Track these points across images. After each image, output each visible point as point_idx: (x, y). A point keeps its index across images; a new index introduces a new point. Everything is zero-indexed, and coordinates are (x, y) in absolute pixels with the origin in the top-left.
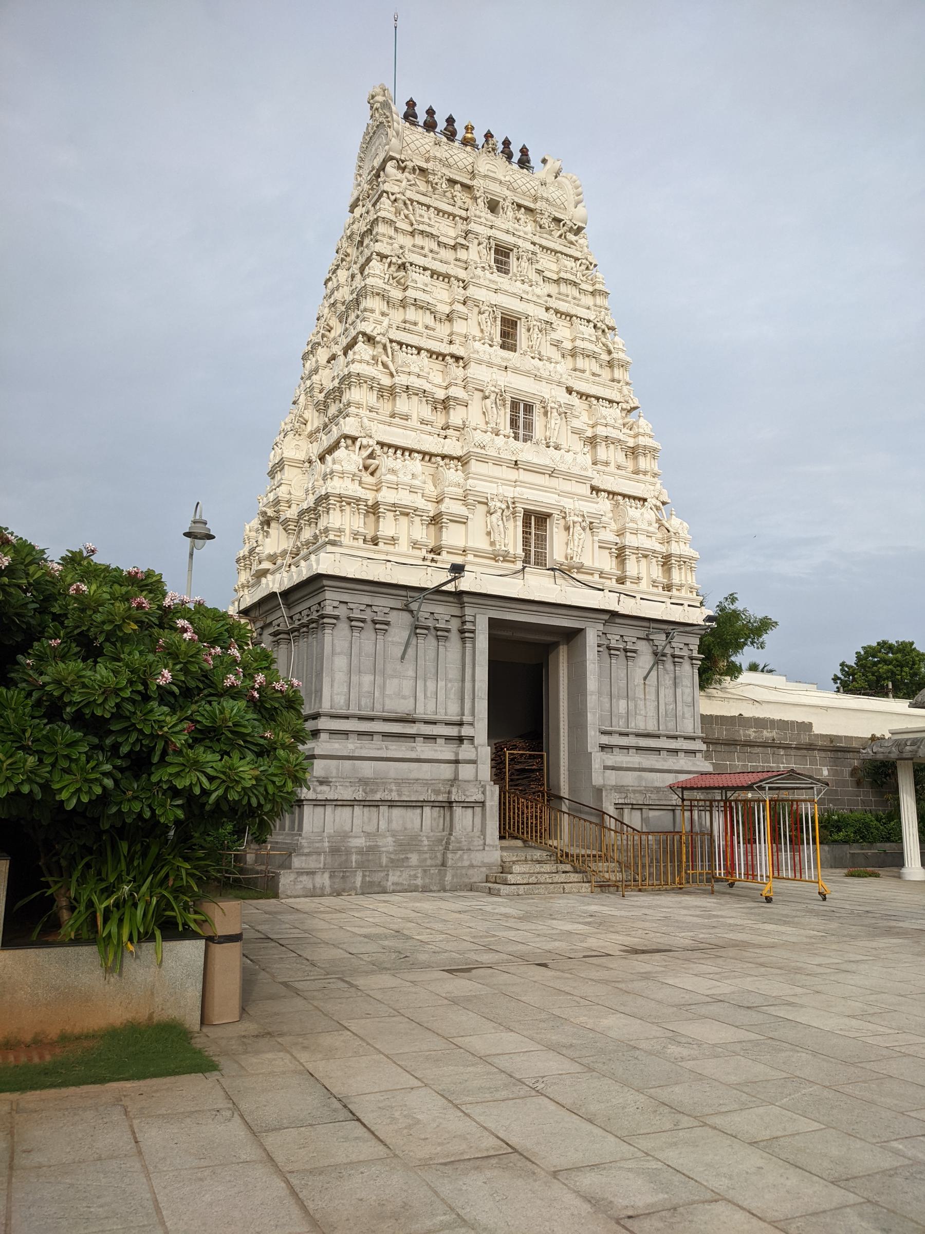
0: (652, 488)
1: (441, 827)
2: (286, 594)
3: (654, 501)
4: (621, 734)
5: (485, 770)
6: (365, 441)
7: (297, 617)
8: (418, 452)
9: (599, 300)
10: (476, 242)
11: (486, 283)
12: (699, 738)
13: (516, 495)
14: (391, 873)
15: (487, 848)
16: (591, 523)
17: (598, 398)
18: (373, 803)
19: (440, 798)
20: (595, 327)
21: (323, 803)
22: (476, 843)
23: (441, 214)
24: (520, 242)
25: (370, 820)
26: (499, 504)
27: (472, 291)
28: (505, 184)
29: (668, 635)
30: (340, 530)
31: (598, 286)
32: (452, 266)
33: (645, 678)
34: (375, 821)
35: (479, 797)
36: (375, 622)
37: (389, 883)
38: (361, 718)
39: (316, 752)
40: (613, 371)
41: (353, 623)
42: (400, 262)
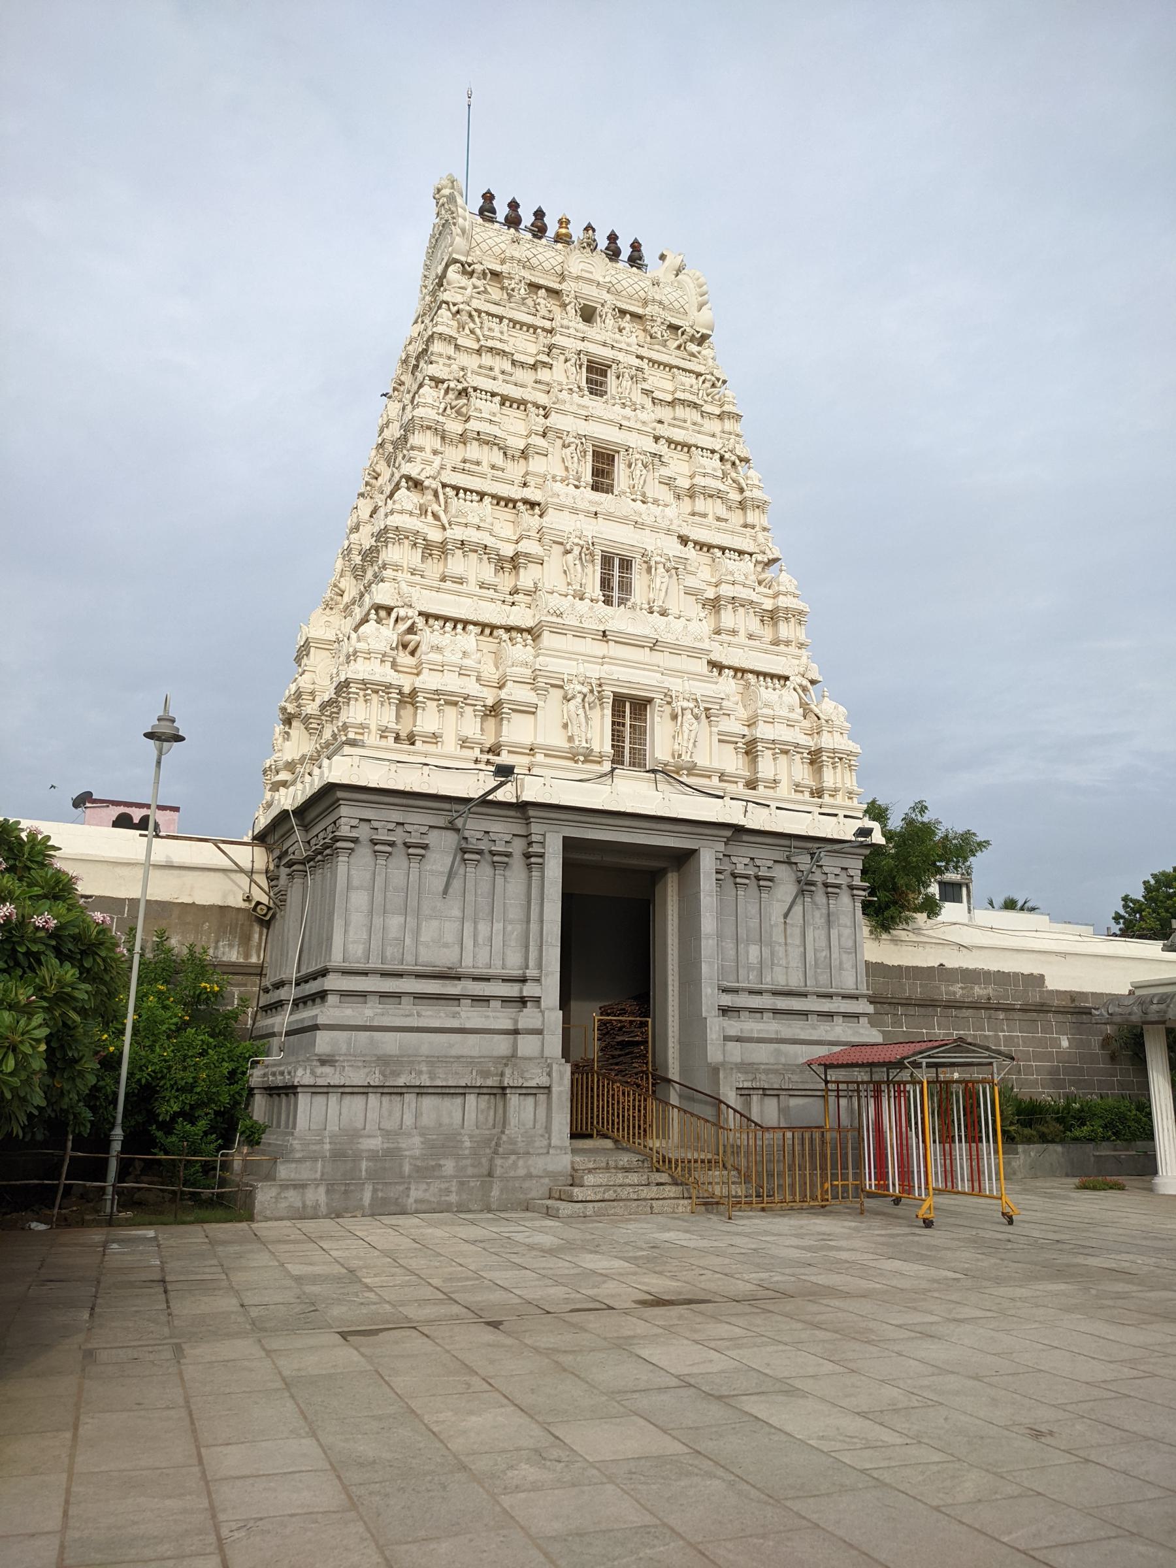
0: (797, 662)
1: (491, 1121)
2: (301, 811)
3: (799, 680)
4: (752, 992)
6: (402, 612)
7: (313, 842)
8: (475, 624)
9: (729, 425)
10: (562, 358)
11: (574, 409)
12: (863, 996)
13: (603, 675)
14: (413, 1187)
15: (551, 1151)
16: (707, 709)
17: (723, 549)
18: (396, 1090)
19: (489, 1082)
20: (722, 459)
21: (325, 1090)
22: (537, 1144)
23: (518, 326)
24: (620, 356)
25: (390, 1113)
26: (579, 688)
27: (555, 420)
28: (604, 286)
29: (812, 855)
30: (363, 726)
31: (726, 408)
32: (529, 389)
33: (786, 916)
34: (398, 1114)
35: (543, 1081)
36: (407, 846)
38: (385, 974)
39: (320, 1021)
40: (745, 514)
41: (377, 848)
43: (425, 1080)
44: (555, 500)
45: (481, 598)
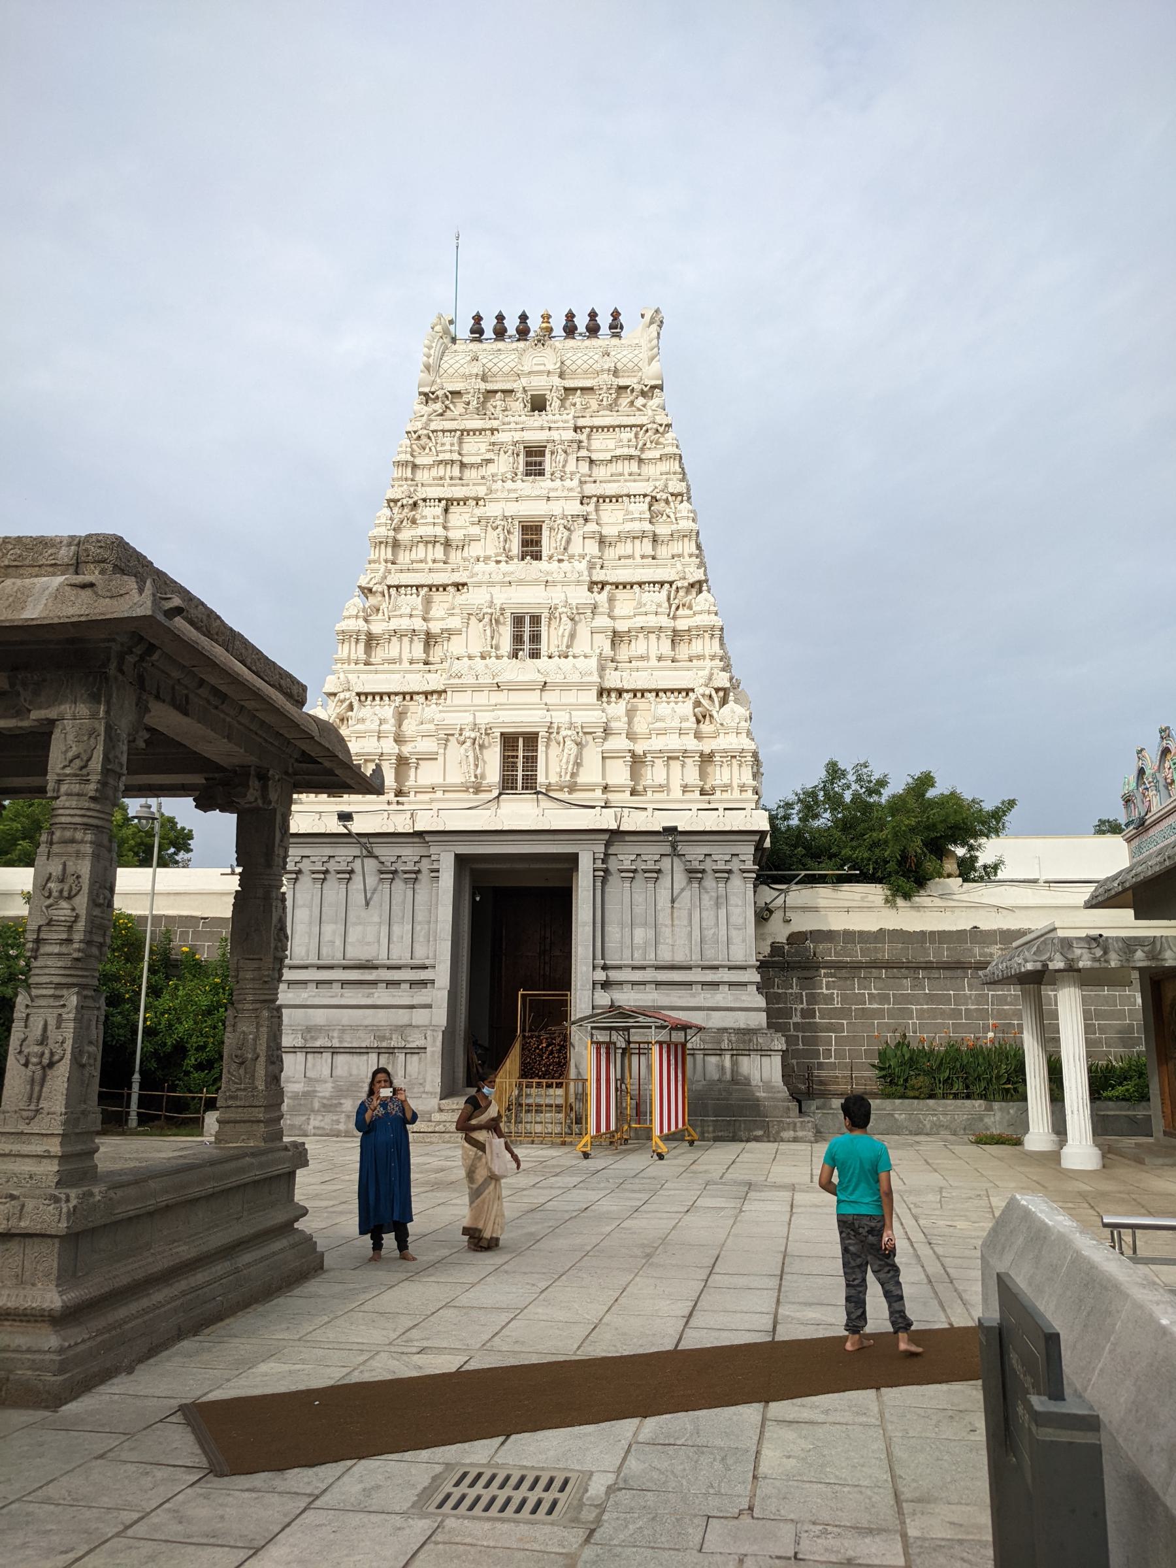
5: (440, 1016)
14: (312, 1117)
19: (384, 1044)
22: (415, 1090)
24: (555, 435)
25: (314, 1065)
33: (673, 901)
38: (319, 968)
42: (411, 501)
44: (474, 579)
45: (410, 672)
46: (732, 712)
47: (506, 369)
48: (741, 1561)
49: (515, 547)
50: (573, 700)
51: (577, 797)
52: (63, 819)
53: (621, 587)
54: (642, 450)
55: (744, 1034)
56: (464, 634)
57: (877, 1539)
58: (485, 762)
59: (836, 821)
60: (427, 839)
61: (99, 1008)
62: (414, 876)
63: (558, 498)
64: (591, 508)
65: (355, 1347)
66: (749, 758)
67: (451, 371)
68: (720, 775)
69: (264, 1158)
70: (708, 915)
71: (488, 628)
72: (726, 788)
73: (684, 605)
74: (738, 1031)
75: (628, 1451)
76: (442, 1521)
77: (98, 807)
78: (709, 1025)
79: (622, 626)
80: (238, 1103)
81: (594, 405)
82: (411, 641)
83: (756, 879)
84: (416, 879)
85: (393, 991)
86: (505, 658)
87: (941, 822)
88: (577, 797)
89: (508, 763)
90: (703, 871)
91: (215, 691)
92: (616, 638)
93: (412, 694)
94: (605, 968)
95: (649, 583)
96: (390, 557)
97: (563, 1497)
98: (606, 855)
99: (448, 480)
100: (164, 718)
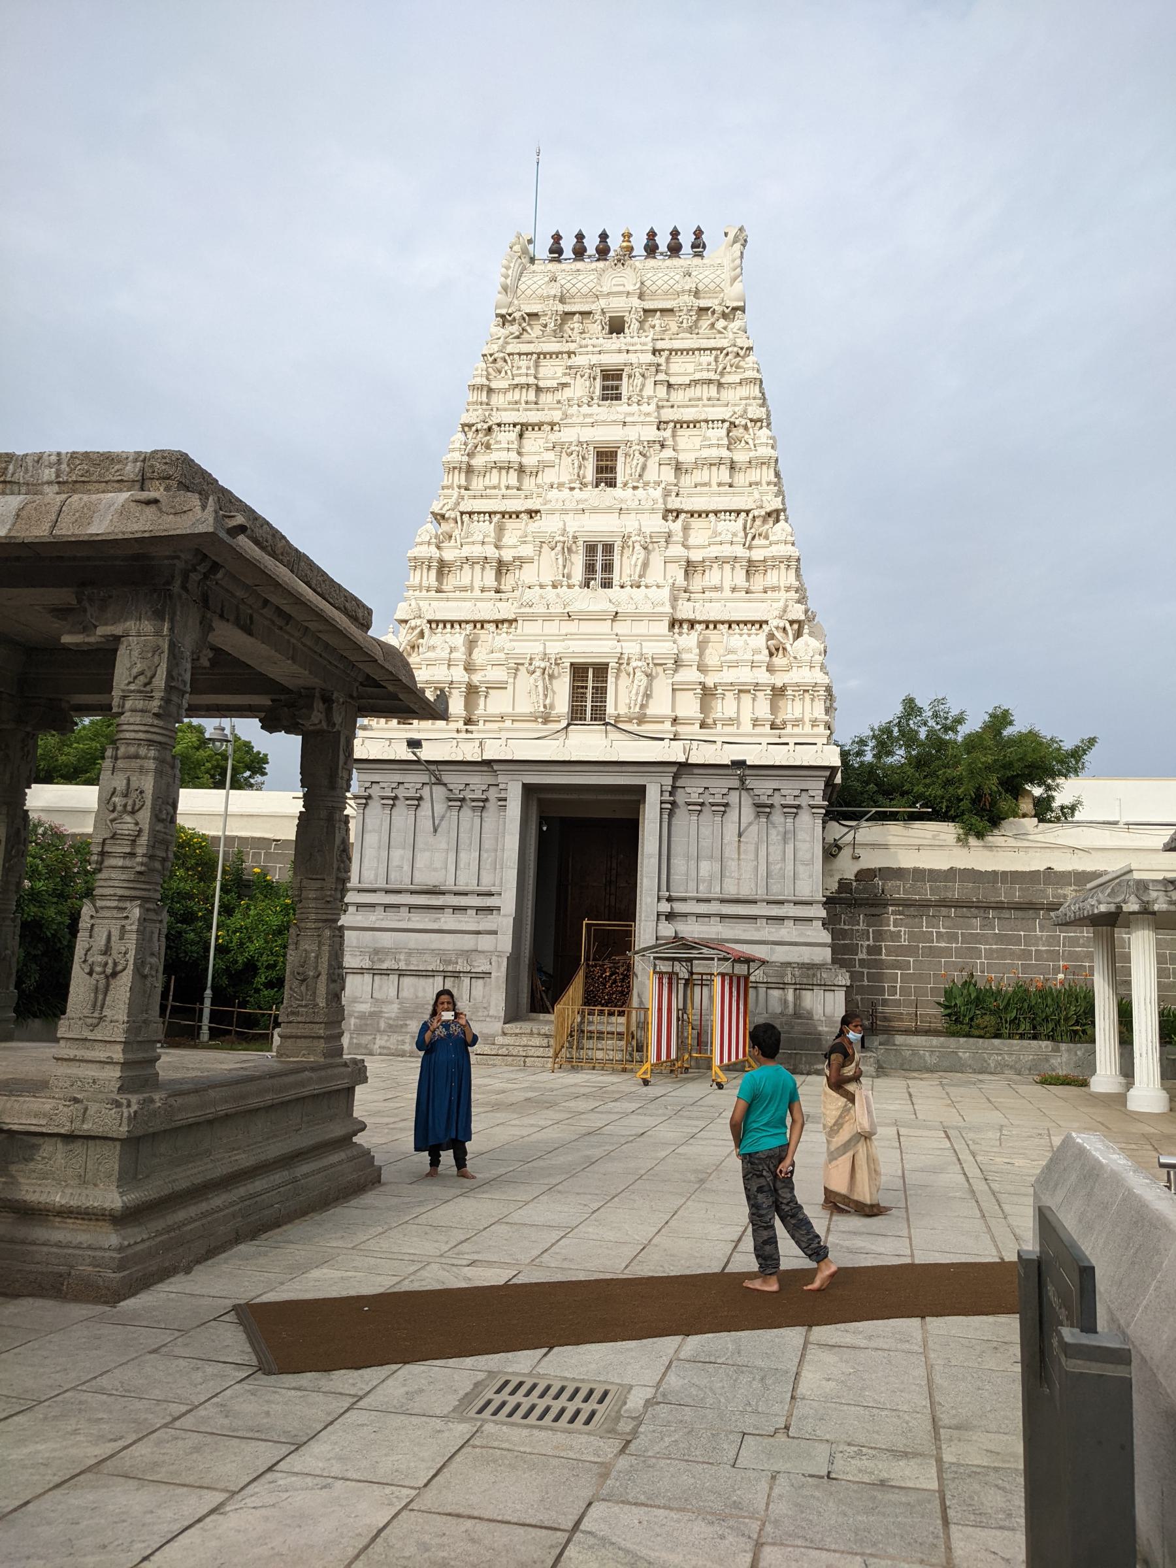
5: (505, 943)
12: (818, 902)
14: (378, 1037)
19: (450, 968)
24: (632, 358)
25: (381, 987)
33: (740, 835)
37: (377, 1046)
38: (387, 892)
42: (486, 426)
43: (402, 966)
45: (481, 600)
46: (807, 645)
47: (585, 290)
48: (773, 1478)
49: (590, 473)
50: (645, 632)
51: (647, 728)
52: (128, 735)
53: (696, 515)
54: (722, 374)
55: (808, 969)
56: (536, 563)
57: (912, 1462)
58: (554, 693)
59: (909, 758)
60: (495, 768)
61: (161, 921)
62: (481, 804)
63: (634, 423)
64: (668, 434)
65: (407, 1257)
66: (822, 693)
67: (529, 292)
68: (792, 709)
69: (323, 1073)
70: (776, 851)
71: (560, 556)
72: (797, 722)
73: (760, 535)
74: (803, 966)
75: (669, 1367)
76: (481, 1426)
77: (161, 723)
78: (773, 959)
79: (696, 556)
80: (299, 1019)
81: (674, 327)
82: (483, 569)
83: (825, 815)
84: (483, 807)
85: (459, 916)
86: (577, 588)
87: (1019, 760)
88: (647, 728)
89: (577, 694)
90: (771, 806)
91: (279, 611)
92: (690, 568)
93: (483, 623)
94: (669, 899)
95: (725, 511)
96: (463, 483)
97: (601, 1408)
98: (674, 787)
99: (524, 405)
100: (228, 637)
